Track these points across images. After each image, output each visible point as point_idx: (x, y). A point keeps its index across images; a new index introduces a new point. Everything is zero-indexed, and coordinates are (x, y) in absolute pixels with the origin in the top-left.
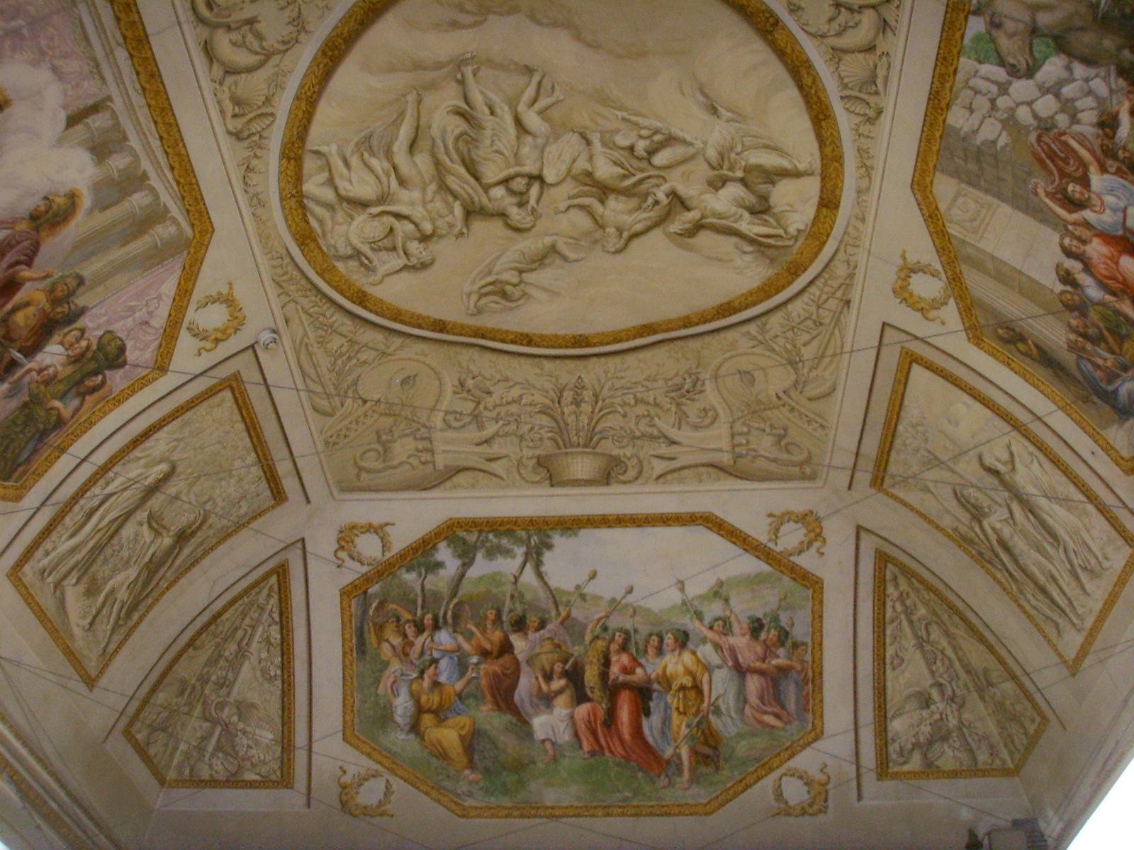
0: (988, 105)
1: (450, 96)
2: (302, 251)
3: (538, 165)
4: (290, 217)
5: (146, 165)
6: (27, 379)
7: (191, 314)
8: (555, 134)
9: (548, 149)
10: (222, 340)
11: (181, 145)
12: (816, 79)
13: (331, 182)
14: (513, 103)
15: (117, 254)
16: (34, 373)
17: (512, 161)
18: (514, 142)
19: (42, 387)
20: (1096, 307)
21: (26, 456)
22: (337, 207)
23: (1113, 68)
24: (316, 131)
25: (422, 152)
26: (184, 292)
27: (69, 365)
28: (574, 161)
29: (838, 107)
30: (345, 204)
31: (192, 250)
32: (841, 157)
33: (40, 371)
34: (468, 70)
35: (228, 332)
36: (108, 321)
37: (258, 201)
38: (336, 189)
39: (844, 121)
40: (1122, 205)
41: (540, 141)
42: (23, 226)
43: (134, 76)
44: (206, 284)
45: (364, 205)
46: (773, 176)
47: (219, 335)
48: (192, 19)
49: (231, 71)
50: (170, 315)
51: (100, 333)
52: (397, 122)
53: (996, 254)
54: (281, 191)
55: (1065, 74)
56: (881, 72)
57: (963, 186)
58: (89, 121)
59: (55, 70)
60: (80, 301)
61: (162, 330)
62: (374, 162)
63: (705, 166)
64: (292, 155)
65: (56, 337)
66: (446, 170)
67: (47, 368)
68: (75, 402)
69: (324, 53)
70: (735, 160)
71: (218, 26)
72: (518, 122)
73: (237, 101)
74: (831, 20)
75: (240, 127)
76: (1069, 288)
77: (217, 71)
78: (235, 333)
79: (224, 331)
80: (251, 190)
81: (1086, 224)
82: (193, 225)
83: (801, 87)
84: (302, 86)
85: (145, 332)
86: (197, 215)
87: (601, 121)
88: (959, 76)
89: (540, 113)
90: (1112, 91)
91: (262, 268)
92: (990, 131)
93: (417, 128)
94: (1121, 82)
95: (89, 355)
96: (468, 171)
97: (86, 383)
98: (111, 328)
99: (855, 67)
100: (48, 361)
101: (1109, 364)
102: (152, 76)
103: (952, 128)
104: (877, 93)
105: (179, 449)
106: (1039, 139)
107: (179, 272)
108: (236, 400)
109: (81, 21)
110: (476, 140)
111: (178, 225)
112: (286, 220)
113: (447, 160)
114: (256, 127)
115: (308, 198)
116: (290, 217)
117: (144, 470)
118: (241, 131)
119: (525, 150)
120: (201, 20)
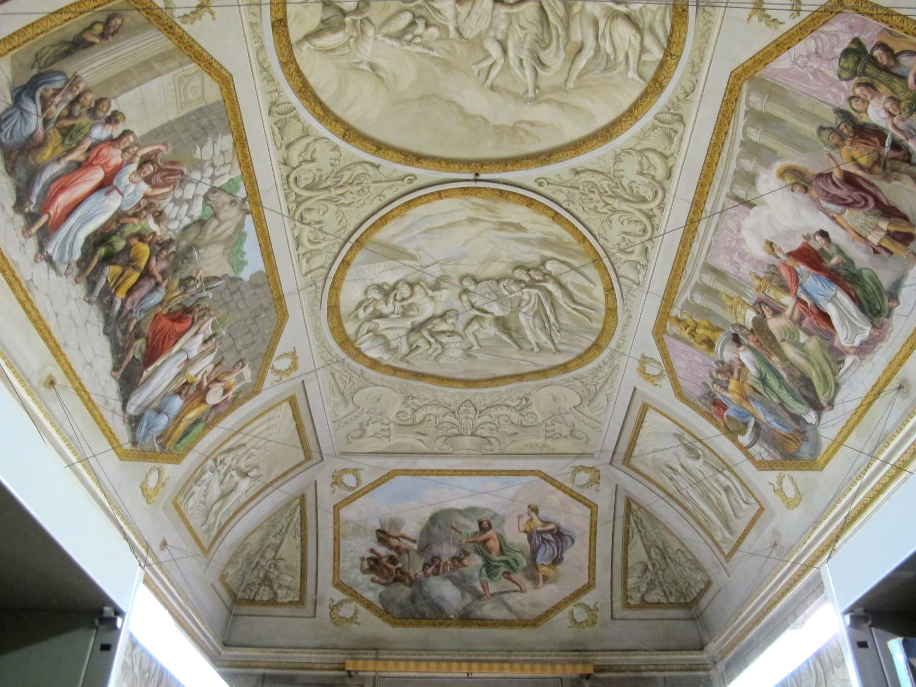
0: (216, 163)
1: (548, 78)
3: (496, 13)
4: (681, 40)
5: (737, 149)
6: (901, 125)
8: (480, 37)
9: (487, 26)
12: (313, 112)
13: (643, 50)
14: (506, 67)
15: (791, 119)
16: (895, 120)
17: (514, 18)
18: (510, 35)
19: (903, 105)
20: (88, 127)
22: (646, 28)
23: (174, 238)
24: (636, 94)
25: (576, 43)
27: (877, 91)
28: (469, 13)
29: (295, 101)
30: (641, 26)
31: (752, 72)
32: (282, 68)
33: (892, 115)
34: (531, 94)
36: (833, 85)
37: (694, 69)
38: (642, 43)
39: (290, 95)
40: (125, 195)
41: (492, 34)
42: (813, 193)
45: (628, 17)
46: (326, 27)
49: (665, 157)
50: (800, 40)
51: (844, 83)
52: (585, 71)
53: (158, 81)
54: (676, 64)
55: (191, 213)
56: (278, 136)
57: (203, 104)
58: (743, 197)
59: (739, 231)
60: (832, 119)
61: (814, 34)
62: (609, 50)
63: (373, 20)
64: (658, 85)
65: (863, 119)
66: (562, 21)
69: (611, 136)
70: (353, 31)
71: (658, 182)
72: (505, 51)
73: (670, 139)
74: (315, 150)
75: (677, 124)
76: (109, 114)
77: (671, 162)
80: (694, 79)
81: (130, 162)
82: (740, 88)
83: (321, 103)
84: (631, 125)
86: (733, 93)
87: (447, 47)
88: (237, 164)
89: (488, 56)
90: (169, 230)
92: (205, 152)
93: (573, 62)
94: (167, 238)
95: (864, 79)
96: (547, 17)
98: (837, 78)
99: (294, 131)
100: (883, 114)
101: (53, 108)
102: (702, 186)
103: (226, 134)
104: (276, 123)
106: (182, 173)
110: (537, 42)
111: (747, 97)
112: (685, 39)
113: (560, 32)
114: (668, 117)
115: (663, 47)
118: (678, 121)
119: (503, 26)
120: (664, 189)
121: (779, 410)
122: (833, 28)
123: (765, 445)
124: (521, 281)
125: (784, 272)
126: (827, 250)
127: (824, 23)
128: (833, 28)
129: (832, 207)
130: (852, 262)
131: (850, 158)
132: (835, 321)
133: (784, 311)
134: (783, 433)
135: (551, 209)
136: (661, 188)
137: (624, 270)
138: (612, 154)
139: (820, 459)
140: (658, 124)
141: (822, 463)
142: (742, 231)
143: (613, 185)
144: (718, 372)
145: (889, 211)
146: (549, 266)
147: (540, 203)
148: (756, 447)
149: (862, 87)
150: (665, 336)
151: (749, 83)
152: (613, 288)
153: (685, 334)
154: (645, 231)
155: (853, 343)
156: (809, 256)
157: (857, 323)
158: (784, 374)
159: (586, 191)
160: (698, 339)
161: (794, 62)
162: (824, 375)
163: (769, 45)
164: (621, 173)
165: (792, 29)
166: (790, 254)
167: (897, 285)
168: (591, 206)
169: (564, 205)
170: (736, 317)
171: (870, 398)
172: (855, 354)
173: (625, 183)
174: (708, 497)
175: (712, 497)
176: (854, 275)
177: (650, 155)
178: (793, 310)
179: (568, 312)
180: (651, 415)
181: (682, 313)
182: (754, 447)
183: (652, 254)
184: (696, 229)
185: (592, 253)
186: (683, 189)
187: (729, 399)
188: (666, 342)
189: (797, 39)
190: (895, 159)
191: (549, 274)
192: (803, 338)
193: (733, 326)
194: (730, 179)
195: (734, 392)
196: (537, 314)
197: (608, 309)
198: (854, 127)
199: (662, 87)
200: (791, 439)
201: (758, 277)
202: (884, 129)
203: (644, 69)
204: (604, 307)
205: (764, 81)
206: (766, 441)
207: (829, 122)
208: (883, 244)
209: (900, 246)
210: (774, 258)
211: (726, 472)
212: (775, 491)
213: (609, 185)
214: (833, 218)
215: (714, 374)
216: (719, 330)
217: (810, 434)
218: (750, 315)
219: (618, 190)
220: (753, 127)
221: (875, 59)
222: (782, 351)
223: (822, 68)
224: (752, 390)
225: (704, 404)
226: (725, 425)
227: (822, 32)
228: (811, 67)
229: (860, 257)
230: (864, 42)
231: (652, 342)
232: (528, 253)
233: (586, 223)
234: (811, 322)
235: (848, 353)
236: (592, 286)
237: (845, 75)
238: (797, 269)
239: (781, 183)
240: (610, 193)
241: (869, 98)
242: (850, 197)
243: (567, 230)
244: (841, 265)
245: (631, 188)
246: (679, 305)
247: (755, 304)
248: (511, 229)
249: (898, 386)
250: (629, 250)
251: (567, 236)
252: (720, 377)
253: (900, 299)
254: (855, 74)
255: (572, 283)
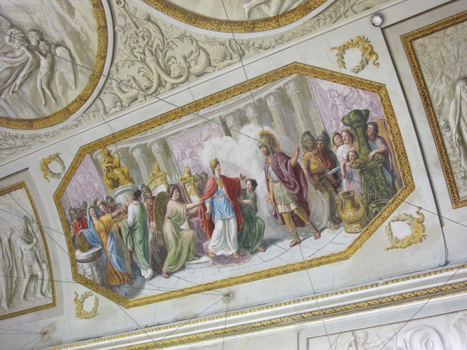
2: (315, 8)
4: (291, 20)
6: (348, 168)
7: (348, 72)
10: (372, 49)
11: (245, 83)
15: (298, 114)
16: (347, 164)
19: (358, 160)
21: (390, 178)
26: (332, 76)
27: (353, 143)
31: (305, 73)
33: (348, 160)
35: (366, 46)
36: (336, 119)
37: (280, 40)
43: (212, 106)
44: (329, 63)
47: (368, 52)
48: (187, 83)
50: (344, 84)
51: (341, 124)
54: (274, 28)
58: (229, 126)
59: (206, 140)
60: (318, 134)
61: (353, 88)
65: (333, 149)
67: (348, 156)
68: (378, 142)
69: (194, 23)
71: (189, 72)
73: (224, 58)
75: (237, 55)
77: (209, 69)
78: (369, 42)
79: (365, 49)
82: (290, 74)
85: (350, 98)
91: (324, 31)
95: (353, 132)
97: (369, 135)
98: (341, 118)
100: (345, 156)
105: (450, 75)
107: (318, 80)
108: (423, 36)
109: (187, 129)
111: (289, 82)
112: (293, 21)
115: (278, 12)
116: (291, 20)
117: (453, 101)
118: (239, 54)
120: (187, 79)
121: (127, 255)
122: (364, 96)
123: (94, 268)
124: (28, 41)
125: (209, 183)
126: (248, 192)
127: (363, 89)
128: (364, 96)
129: (273, 175)
130: (256, 211)
131: (307, 160)
132: (216, 232)
133: (187, 203)
134: (116, 269)
135: (105, 21)
136: (187, 76)
137: (107, 98)
138: (182, 32)
139: (132, 301)
140: (227, 45)
141: (131, 304)
142: (208, 142)
143: (161, 47)
144: (103, 203)
145: (302, 203)
146: (59, 51)
147: (104, 12)
148: (86, 265)
149: (348, 134)
150: (88, 156)
151: (297, 77)
152: (86, 101)
153: (104, 166)
154: (148, 89)
155: (217, 252)
156: (234, 188)
157: (229, 243)
158: (150, 237)
159: (140, 35)
160: (110, 175)
161: (330, 91)
162: (180, 255)
163: (327, 70)
164: (174, 46)
165: (347, 75)
166: (223, 177)
167: (273, 241)
168: (133, 45)
169: (116, 28)
170: (151, 183)
171: (201, 288)
172: (212, 258)
173: (170, 53)
174: (11, 272)
175: (15, 274)
176: (252, 218)
177: (203, 55)
178: (194, 207)
179: (36, 88)
180: (20, 194)
181: (116, 152)
182: (84, 264)
183: (136, 105)
184: (181, 117)
185: (98, 70)
186: (200, 89)
187: (94, 225)
188: (85, 159)
189: (344, 82)
190: (330, 181)
191: (53, 55)
192: (185, 226)
193: (143, 186)
194: (232, 110)
195: (103, 223)
196: (12, 69)
197: (67, 109)
198: (324, 148)
199: (253, 30)
200: (119, 277)
201: (189, 173)
202: (338, 163)
203: (256, 11)
204: (65, 105)
205: (307, 83)
206: (97, 266)
207: (315, 133)
208: (284, 215)
209: (292, 224)
210: (211, 171)
211: (44, 266)
212: (75, 300)
213: (158, 45)
214: (268, 181)
215: (99, 203)
216: (131, 180)
217: (137, 282)
218: (163, 188)
219: (160, 53)
220: (275, 98)
221: (367, 128)
222: (163, 224)
223: (339, 107)
224: (117, 231)
225: (70, 214)
226: (75, 236)
227: (357, 92)
228: (335, 101)
229: (264, 211)
230: (370, 116)
231: (75, 151)
232: (57, 30)
233: (117, 50)
234: (198, 222)
235: (208, 254)
236: (73, 88)
237: (346, 121)
238: (219, 188)
239: (258, 138)
240: (153, 50)
241: (345, 142)
242: (288, 178)
243: (99, 42)
244: (248, 207)
245: (169, 60)
246: (119, 147)
247: (172, 185)
248: (64, 7)
249: (227, 293)
250: (124, 89)
251: (94, 45)
252: (101, 207)
253: (268, 250)
254: (351, 125)
255: (62, 73)
